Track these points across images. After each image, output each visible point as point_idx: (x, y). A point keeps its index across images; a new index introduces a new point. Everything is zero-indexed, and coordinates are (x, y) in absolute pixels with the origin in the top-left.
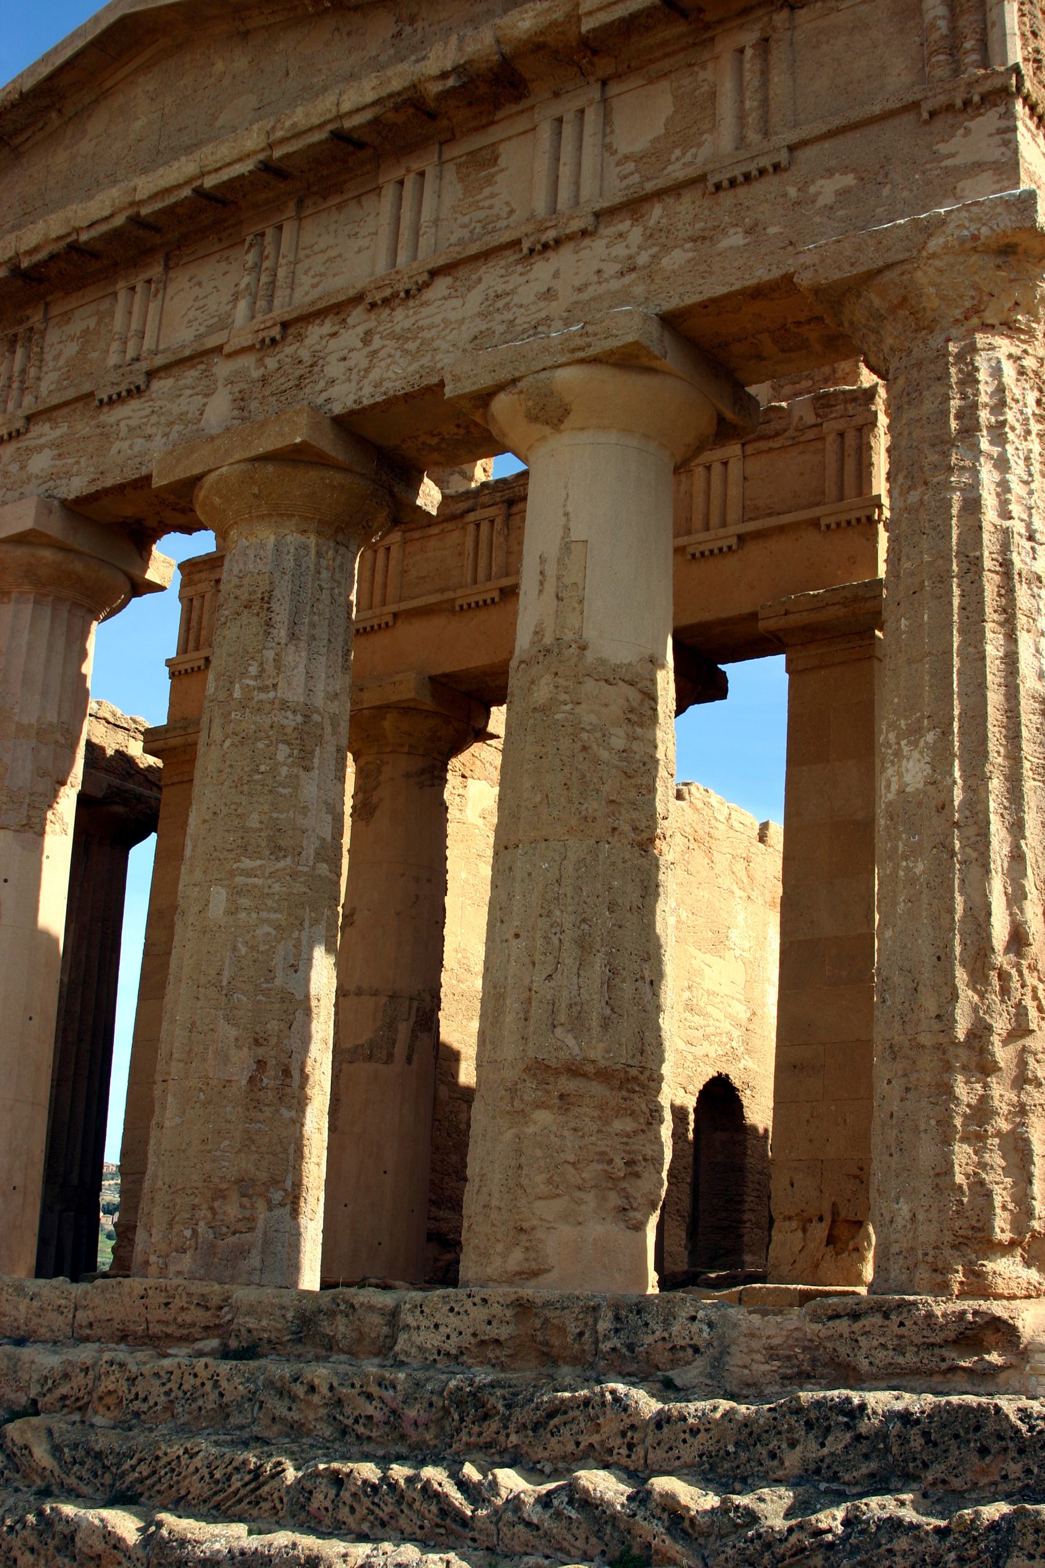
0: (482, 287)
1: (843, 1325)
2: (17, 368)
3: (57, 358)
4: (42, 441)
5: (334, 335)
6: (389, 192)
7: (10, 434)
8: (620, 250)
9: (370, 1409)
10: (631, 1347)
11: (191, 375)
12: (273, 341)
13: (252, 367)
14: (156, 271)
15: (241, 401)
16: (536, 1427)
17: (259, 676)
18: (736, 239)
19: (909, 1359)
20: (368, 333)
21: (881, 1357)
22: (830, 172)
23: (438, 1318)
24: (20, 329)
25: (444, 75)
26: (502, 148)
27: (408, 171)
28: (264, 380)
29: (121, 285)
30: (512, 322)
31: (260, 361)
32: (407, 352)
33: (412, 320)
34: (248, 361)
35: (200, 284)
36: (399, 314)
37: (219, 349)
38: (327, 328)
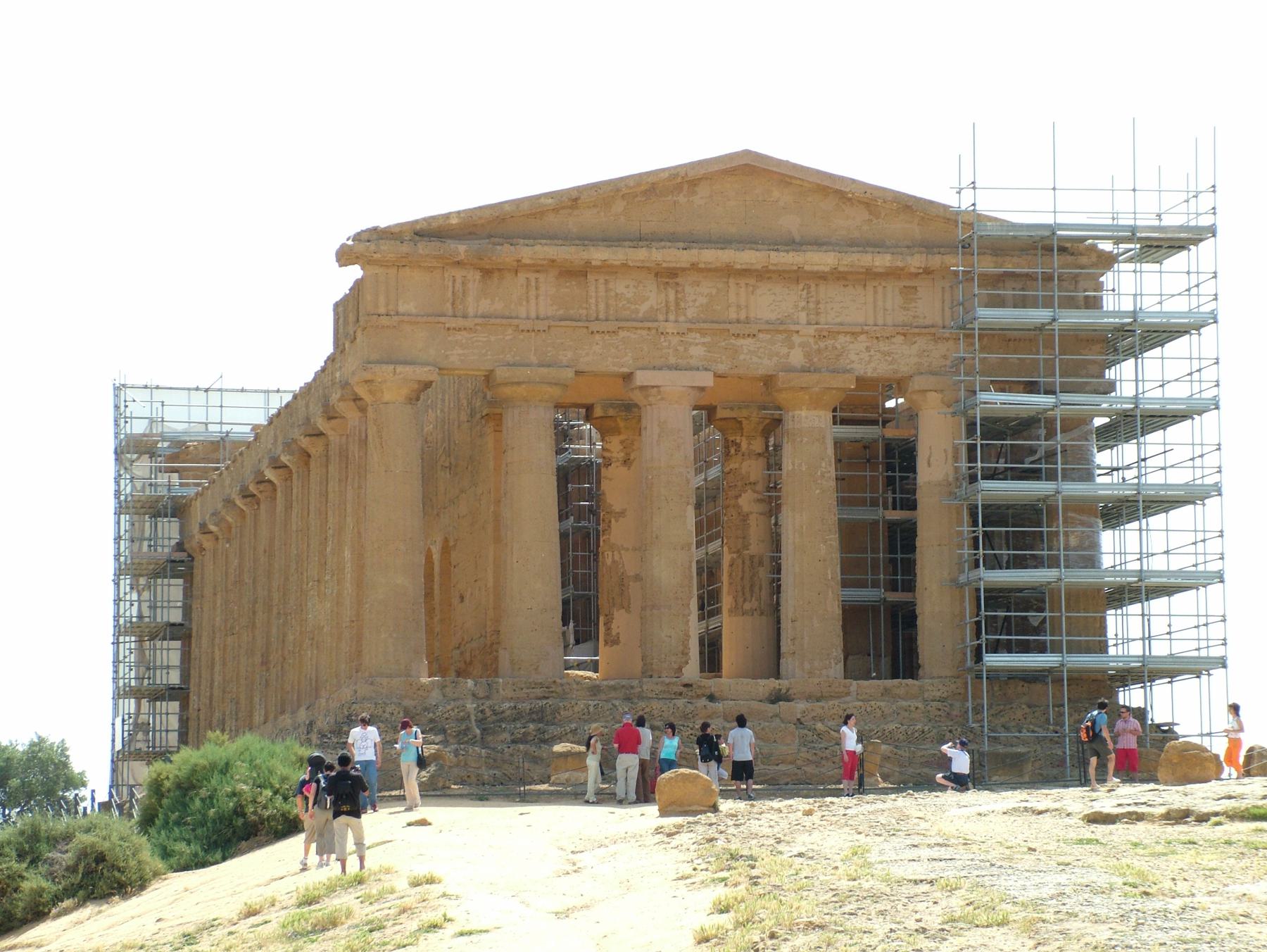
0: (916, 346)
2: (672, 296)
3: (695, 301)
4: (697, 341)
5: (853, 342)
6: (870, 288)
7: (678, 333)
9: (939, 713)
10: (1005, 694)
11: (780, 337)
12: (824, 337)
13: (812, 343)
14: (752, 281)
15: (807, 355)
16: (996, 714)
17: (825, 468)
20: (867, 347)
23: (940, 687)
24: (671, 281)
26: (918, 289)
27: (880, 284)
28: (819, 351)
29: (732, 281)
30: (931, 363)
31: (816, 343)
32: (886, 360)
33: (888, 348)
35: (775, 294)
36: (881, 344)
38: (848, 338)
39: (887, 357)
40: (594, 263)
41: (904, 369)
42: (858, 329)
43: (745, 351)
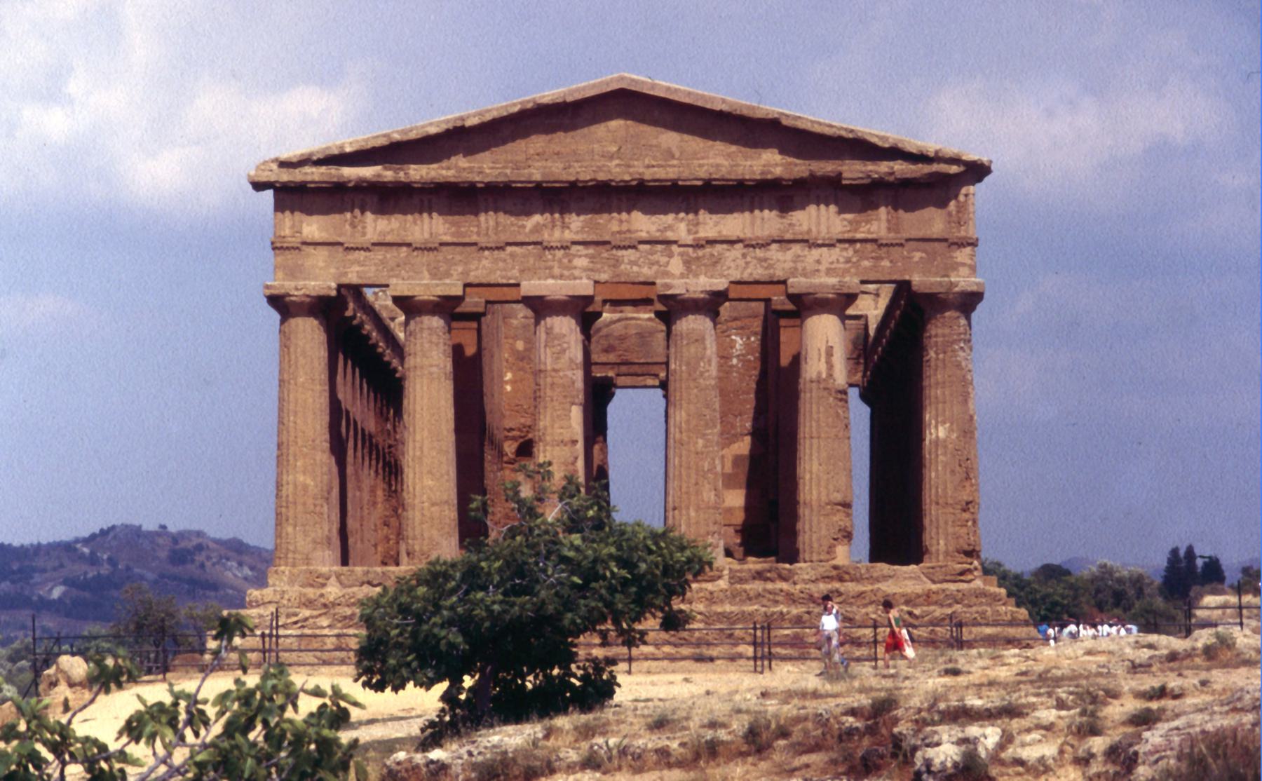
1: (931, 570)
8: (845, 254)
9: (802, 595)
11: (659, 247)
18: (886, 263)
19: (948, 578)
21: (941, 577)
22: (918, 250)
25: (789, 180)
28: (698, 258)
34: (690, 250)
37: (675, 242)
38: (725, 246)
39: (763, 264)
40: (479, 185)
41: (779, 274)
42: (734, 238)
43: (626, 260)
